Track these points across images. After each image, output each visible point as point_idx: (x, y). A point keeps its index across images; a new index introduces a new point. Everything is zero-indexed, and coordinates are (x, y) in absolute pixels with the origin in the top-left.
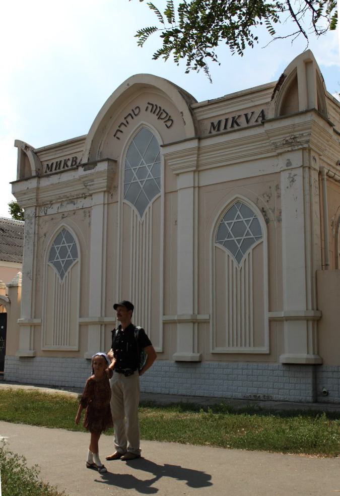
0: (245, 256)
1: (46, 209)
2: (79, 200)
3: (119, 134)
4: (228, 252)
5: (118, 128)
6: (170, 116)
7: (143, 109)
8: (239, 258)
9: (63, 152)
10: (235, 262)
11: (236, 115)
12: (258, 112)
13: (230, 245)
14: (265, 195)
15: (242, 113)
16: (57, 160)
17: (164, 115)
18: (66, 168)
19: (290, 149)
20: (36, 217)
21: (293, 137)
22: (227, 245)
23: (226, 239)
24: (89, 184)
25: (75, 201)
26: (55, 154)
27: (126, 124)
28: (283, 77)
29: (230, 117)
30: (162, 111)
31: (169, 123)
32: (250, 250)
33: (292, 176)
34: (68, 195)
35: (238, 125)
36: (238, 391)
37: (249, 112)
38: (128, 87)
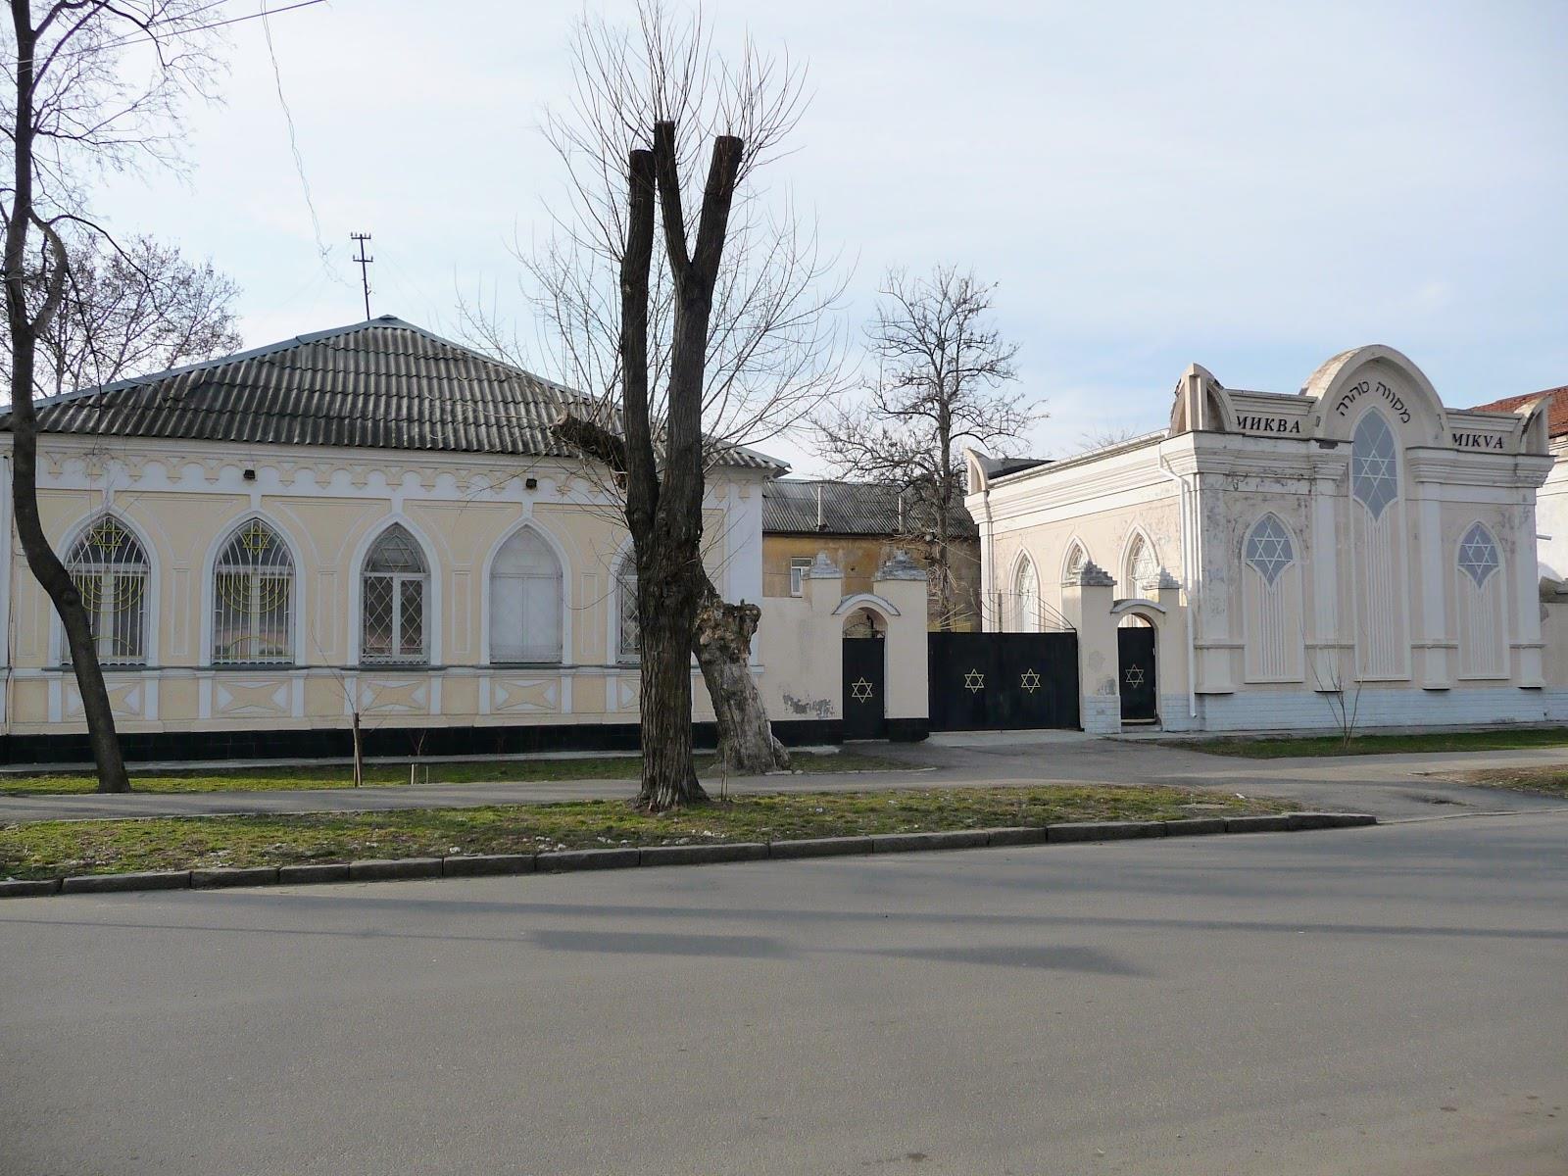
0: (1485, 582)
2: (1290, 482)
4: (1470, 576)
7: (1373, 386)
8: (1480, 584)
9: (1264, 407)
11: (1478, 433)
12: (1497, 436)
13: (1472, 569)
17: (1398, 406)
28: (1532, 414)
31: (1406, 418)
32: (1489, 576)
34: (1279, 471)
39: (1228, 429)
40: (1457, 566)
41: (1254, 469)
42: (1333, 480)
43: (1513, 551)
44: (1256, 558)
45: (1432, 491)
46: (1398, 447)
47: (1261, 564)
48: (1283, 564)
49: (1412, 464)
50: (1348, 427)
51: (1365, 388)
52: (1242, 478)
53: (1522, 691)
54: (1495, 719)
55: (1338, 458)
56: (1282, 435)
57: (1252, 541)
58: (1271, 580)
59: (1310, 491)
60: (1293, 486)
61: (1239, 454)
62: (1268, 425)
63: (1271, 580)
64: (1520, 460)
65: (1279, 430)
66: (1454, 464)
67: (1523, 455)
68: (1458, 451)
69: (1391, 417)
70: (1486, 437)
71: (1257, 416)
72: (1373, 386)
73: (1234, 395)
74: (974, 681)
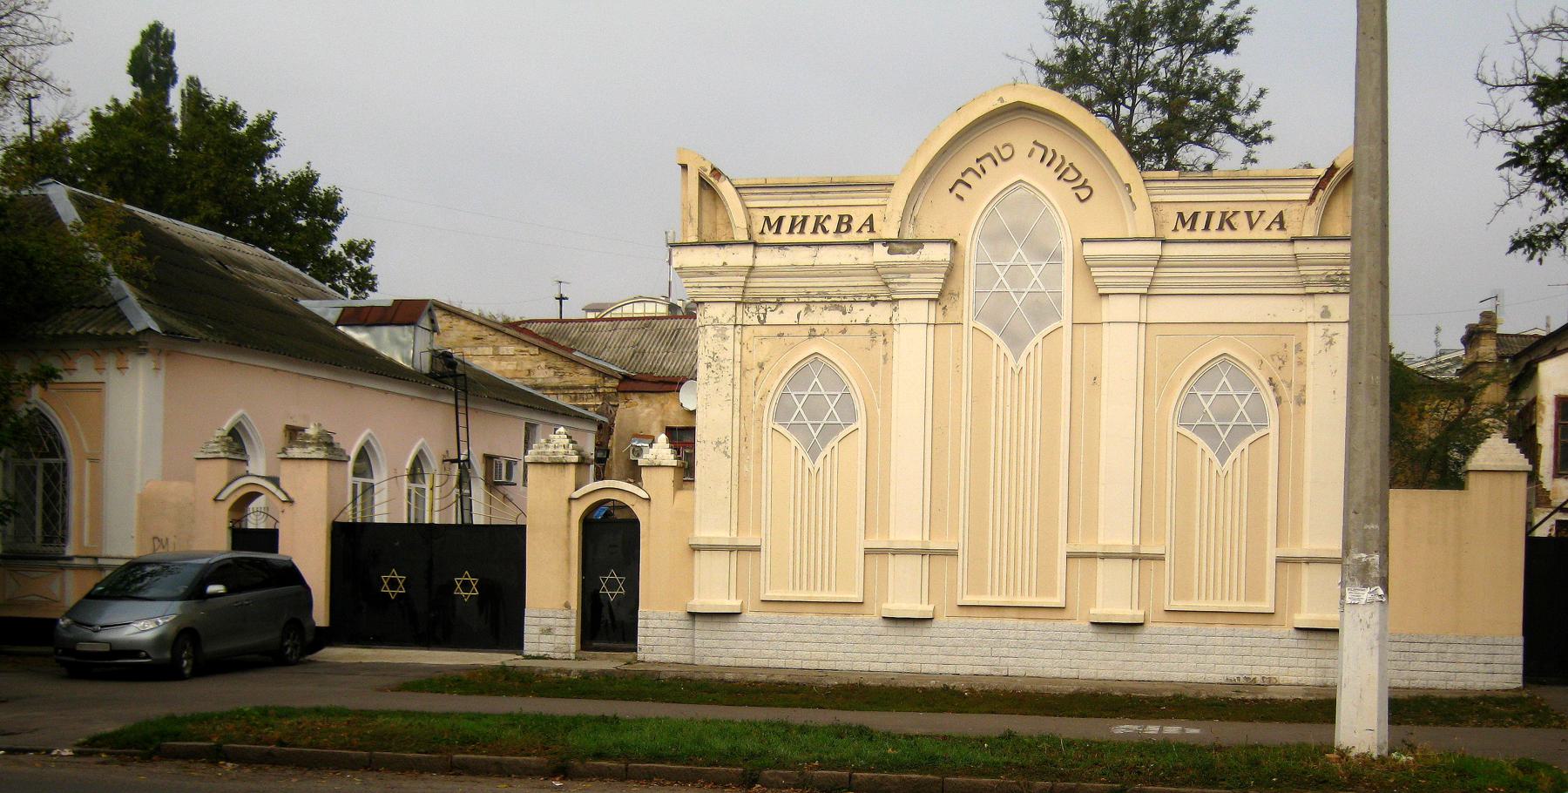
0: (1235, 454)
1: (762, 311)
2: (856, 307)
3: (960, 189)
4: (1201, 443)
5: (960, 177)
6: (1086, 181)
8: (1223, 456)
9: (814, 198)
10: (1216, 461)
11: (1231, 208)
13: (1206, 431)
14: (1276, 358)
15: (1243, 208)
16: (795, 212)
17: (1071, 175)
18: (820, 237)
19: (1331, 290)
20: (735, 325)
21: (1340, 272)
22: (1198, 430)
23: (1198, 422)
24: (895, 281)
25: (848, 307)
27: (980, 172)
29: (1218, 209)
30: (1066, 166)
31: (1084, 193)
32: (1244, 444)
33: (1329, 333)
34: (832, 291)
35: (1232, 228)
36: (1216, 671)
37: (1256, 209)
38: (1000, 105)
43: (1300, 401)
44: (792, 421)
49: (1086, 266)
51: (1006, 153)
52: (773, 307)
53: (1300, 635)
55: (928, 267)
56: (845, 238)
60: (861, 313)
64: (1300, 248)
65: (838, 231)
66: (1160, 262)
69: (1055, 193)
70: (1249, 214)
71: (800, 213)
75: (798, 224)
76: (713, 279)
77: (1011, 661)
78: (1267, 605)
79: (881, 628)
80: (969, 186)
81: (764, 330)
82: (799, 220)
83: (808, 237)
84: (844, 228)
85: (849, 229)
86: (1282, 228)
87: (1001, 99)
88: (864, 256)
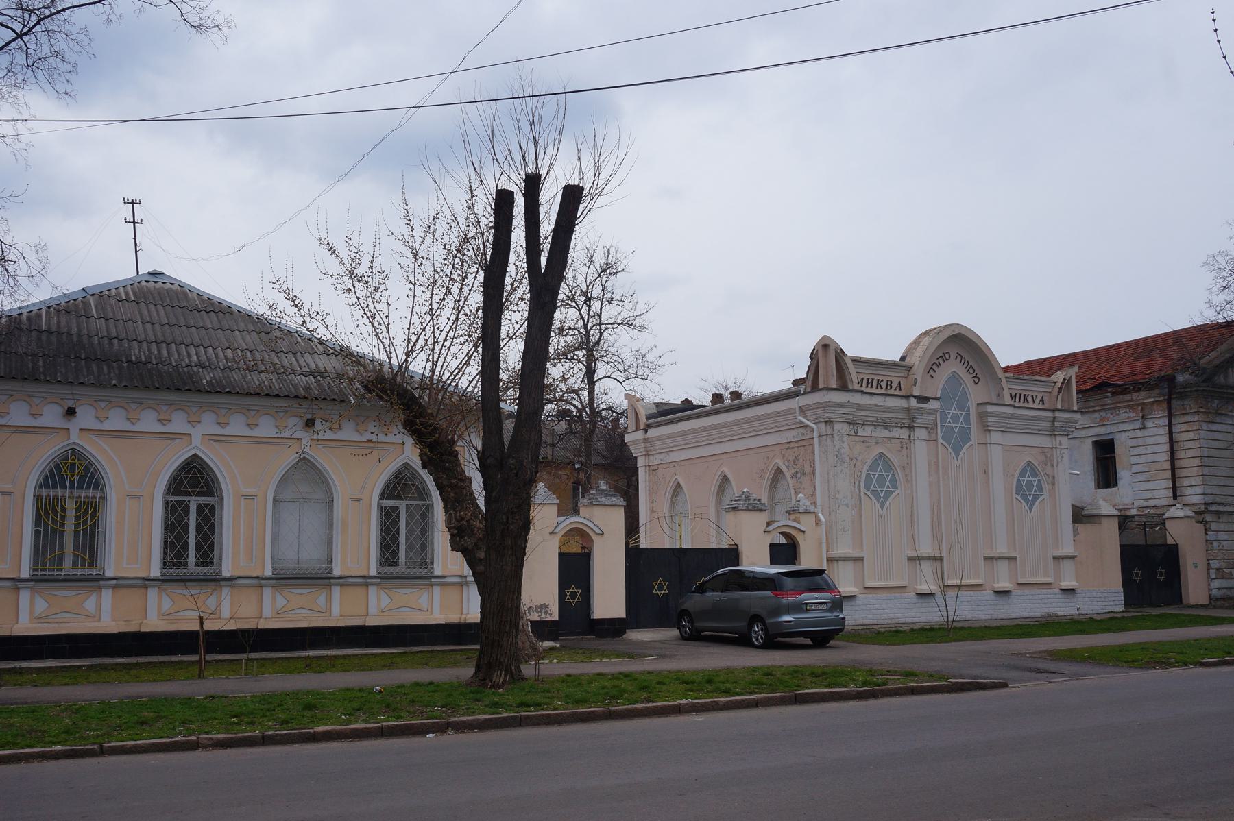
0: (1035, 507)
1: (856, 428)
2: (895, 429)
8: (1031, 508)
13: (1025, 498)
15: (1031, 393)
16: (868, 376)
26: (867, 369)
30: (969, 366)
32: (1037, 503)
34: (888, 420)
37: (1035, 394)
39: (850, 387)
40: (1015, 496)
41: (870, 419)
42: (926, 427)
43: (1053, 484)
45: (996, 437)
46: (972, 403)
47: (875, 493)
48: (891, 492)
49: (982, 416)
50: (935, 387)
54: (1043, 614)
55: (932, 412)
57: (868, 475)
58: (882, 506)
59: (910, 436)
60: (898, 432)
61: (859, 407)
62: (879, 385)
63: (882, 506)
64: (1058, 414)
65: (887, 388)
66: (1010, 416)
67: (1059, 410)
68: (1014, 406)
69: (967, 379)
70: (1032, 396)
71: (871, 377)
72: (953, 355)
73: (858, 361)
74: (661, 587)
75: (870, 383)
76: (841, 409)
77: (966, 613)
78: (1049, 580)
79: (915, 599)
80: (935, 371)
81: (857, 439)
82: (870, 381)
83: (874, 390)
84: (889, 387)
85: (891, 388)
86: (1043, 404)
87: (954, 331)
88: (902, 403)
